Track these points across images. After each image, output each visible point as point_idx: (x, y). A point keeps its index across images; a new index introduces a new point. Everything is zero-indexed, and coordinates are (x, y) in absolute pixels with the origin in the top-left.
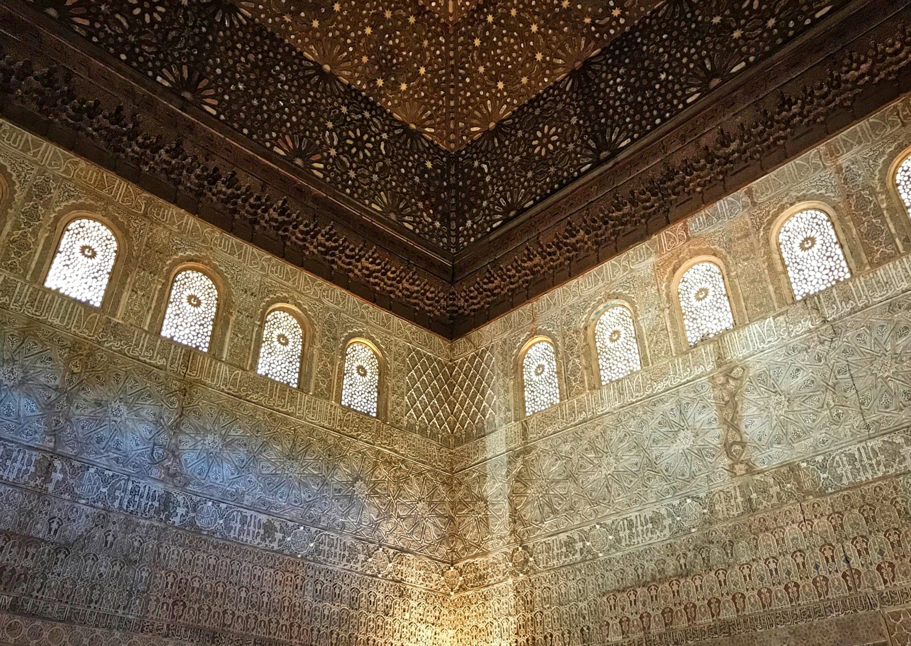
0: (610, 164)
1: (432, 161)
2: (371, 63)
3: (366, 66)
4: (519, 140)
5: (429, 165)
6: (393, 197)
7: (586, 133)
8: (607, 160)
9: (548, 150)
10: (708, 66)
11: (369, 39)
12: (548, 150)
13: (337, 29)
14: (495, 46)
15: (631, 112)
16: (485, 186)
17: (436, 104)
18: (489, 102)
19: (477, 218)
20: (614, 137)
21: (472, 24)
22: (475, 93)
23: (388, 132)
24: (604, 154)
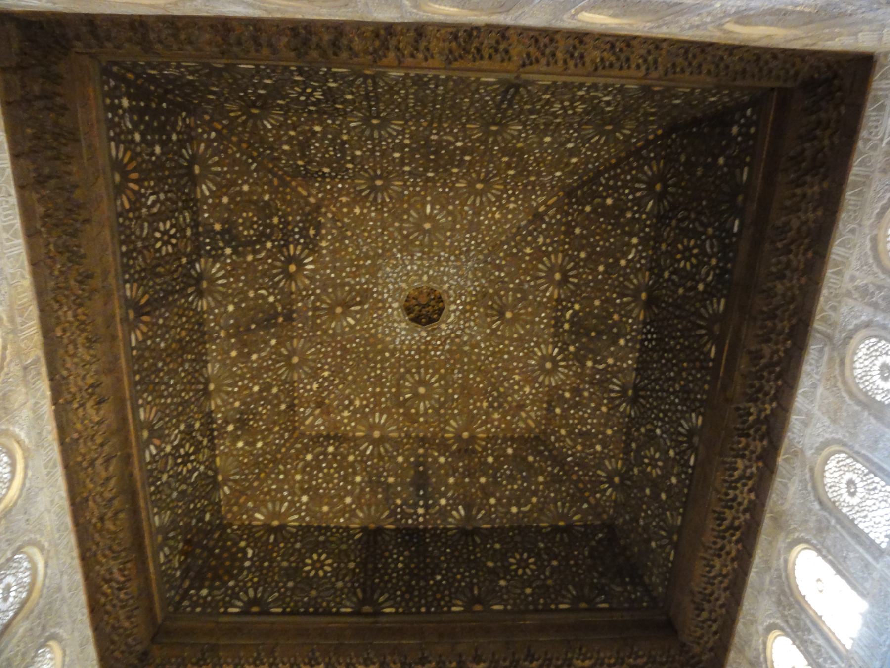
0: (371, 620)
1: (212, 515)
2: (238, 410)
3: (234, 409)
4: (295, 550)
5: (207, 517)
6: (173, 522)
7: (358, 581)
8: (367, 614)
9: (317, 574)
10: (476, 592)
11: (252, 395)
12: (317, 574)
13: (241, 368)
14: (321, 469)
15: (404, 589)
16: (242, 569)
17: (247, 475)
18: (286, 504)
19: (215, 592)
20: (381, 599)
21: (315, 443)
22: (280, 490)
23: (206, 467)
24: (367, 609)
